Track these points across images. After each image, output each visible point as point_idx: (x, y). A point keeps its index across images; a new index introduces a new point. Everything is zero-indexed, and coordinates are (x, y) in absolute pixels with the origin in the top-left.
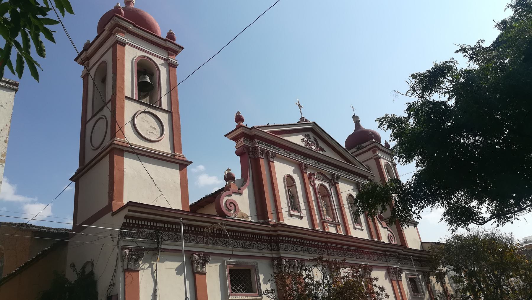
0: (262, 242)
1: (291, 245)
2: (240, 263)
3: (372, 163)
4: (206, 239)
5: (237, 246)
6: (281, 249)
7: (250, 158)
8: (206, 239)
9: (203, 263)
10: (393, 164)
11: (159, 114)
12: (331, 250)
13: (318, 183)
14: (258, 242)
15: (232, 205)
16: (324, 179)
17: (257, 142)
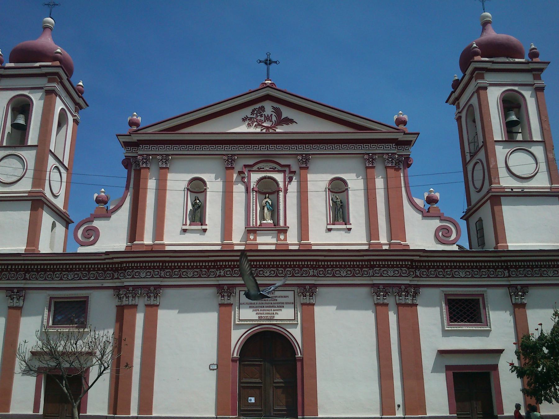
0: (105, 271)
1: (147, 270)
2: (67, 295)
3: (474, 101)
4: (29, 275)
5: (68, 278)
6: (127, 277)
7: (134, 169)
8: (29, 275)
9: (18, 298)
10: (534, 87)
11: (23, 153)
12: (227, 270)
13: (255, 177)
14: (98, 272)
15: (90, 231)
16: (275, 168)
17: (141, 148)
